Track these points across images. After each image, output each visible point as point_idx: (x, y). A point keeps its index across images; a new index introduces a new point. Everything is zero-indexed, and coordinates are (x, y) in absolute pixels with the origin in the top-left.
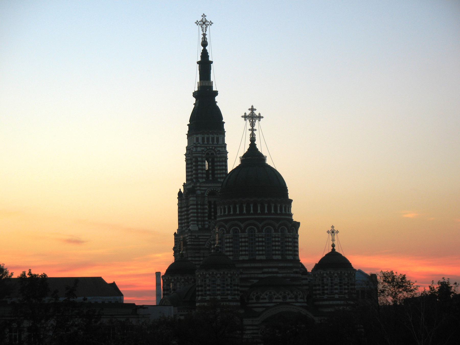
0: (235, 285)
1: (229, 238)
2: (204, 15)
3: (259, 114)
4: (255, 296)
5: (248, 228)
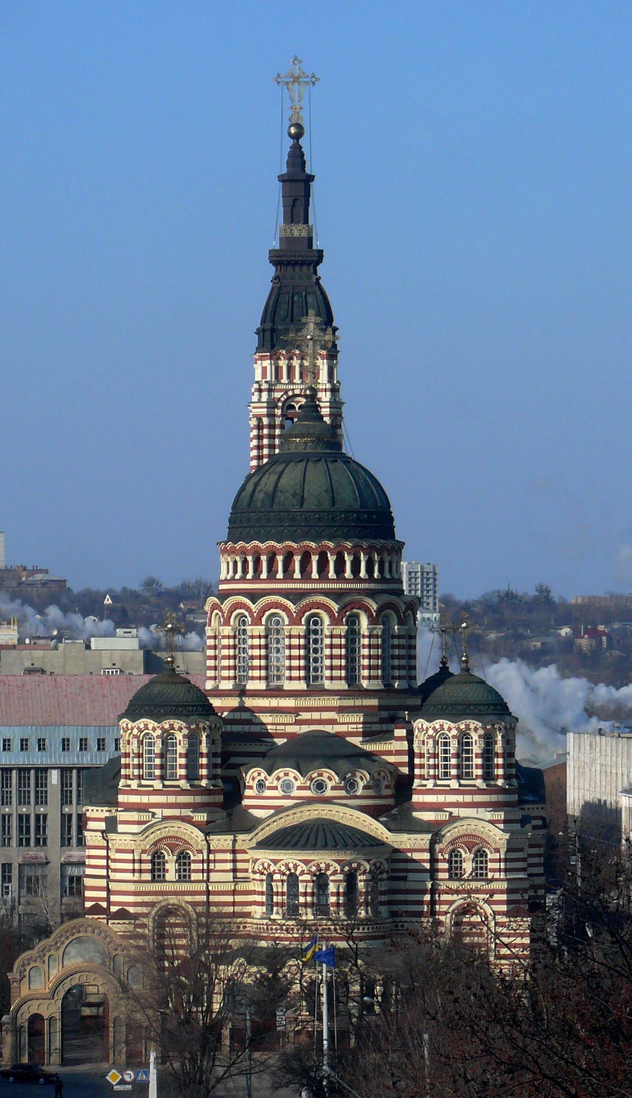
1: (229, 637)
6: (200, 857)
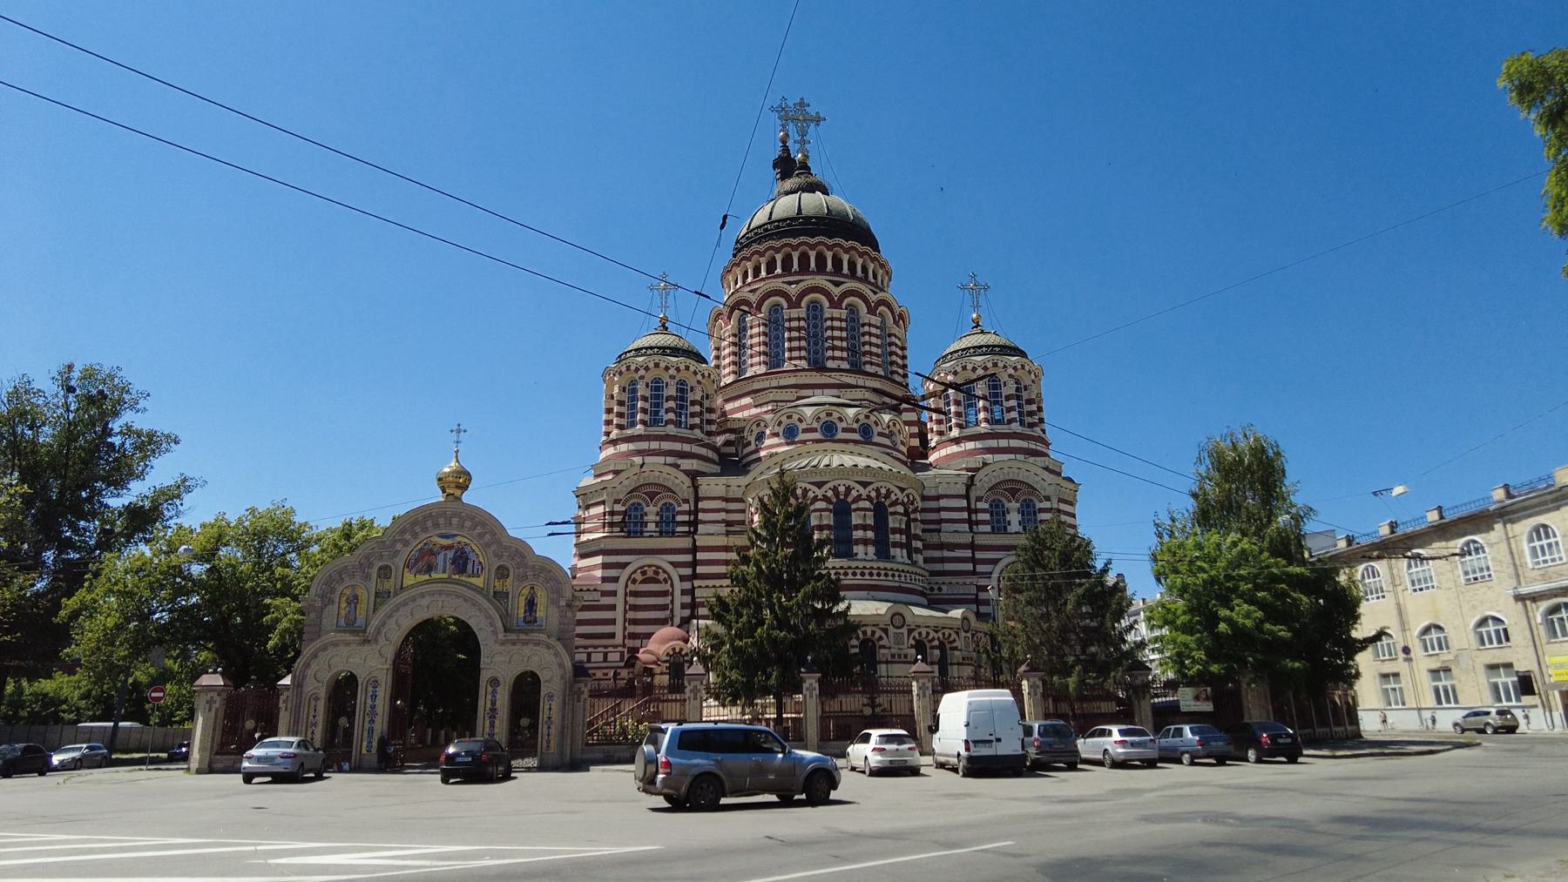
0: (693, 403)
5: (766, 303)
6: (685, 507)
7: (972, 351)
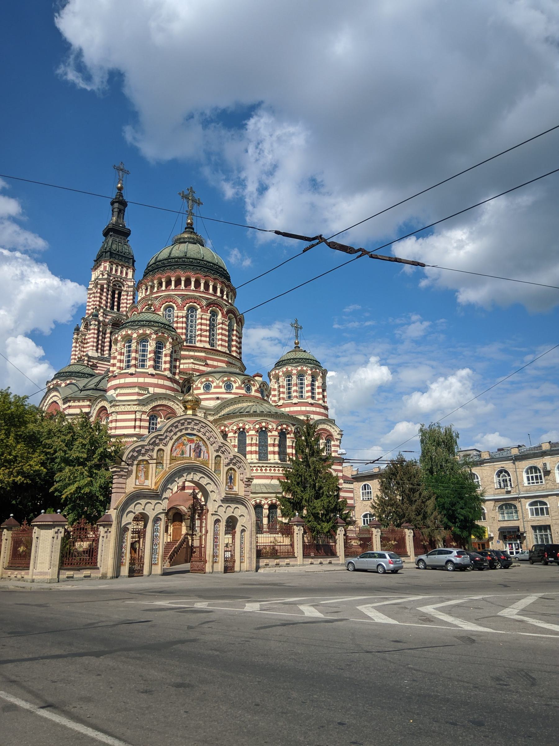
2: (122, 163)
3: (199, 199)
4: (203, 385)
7: (304, 361)
